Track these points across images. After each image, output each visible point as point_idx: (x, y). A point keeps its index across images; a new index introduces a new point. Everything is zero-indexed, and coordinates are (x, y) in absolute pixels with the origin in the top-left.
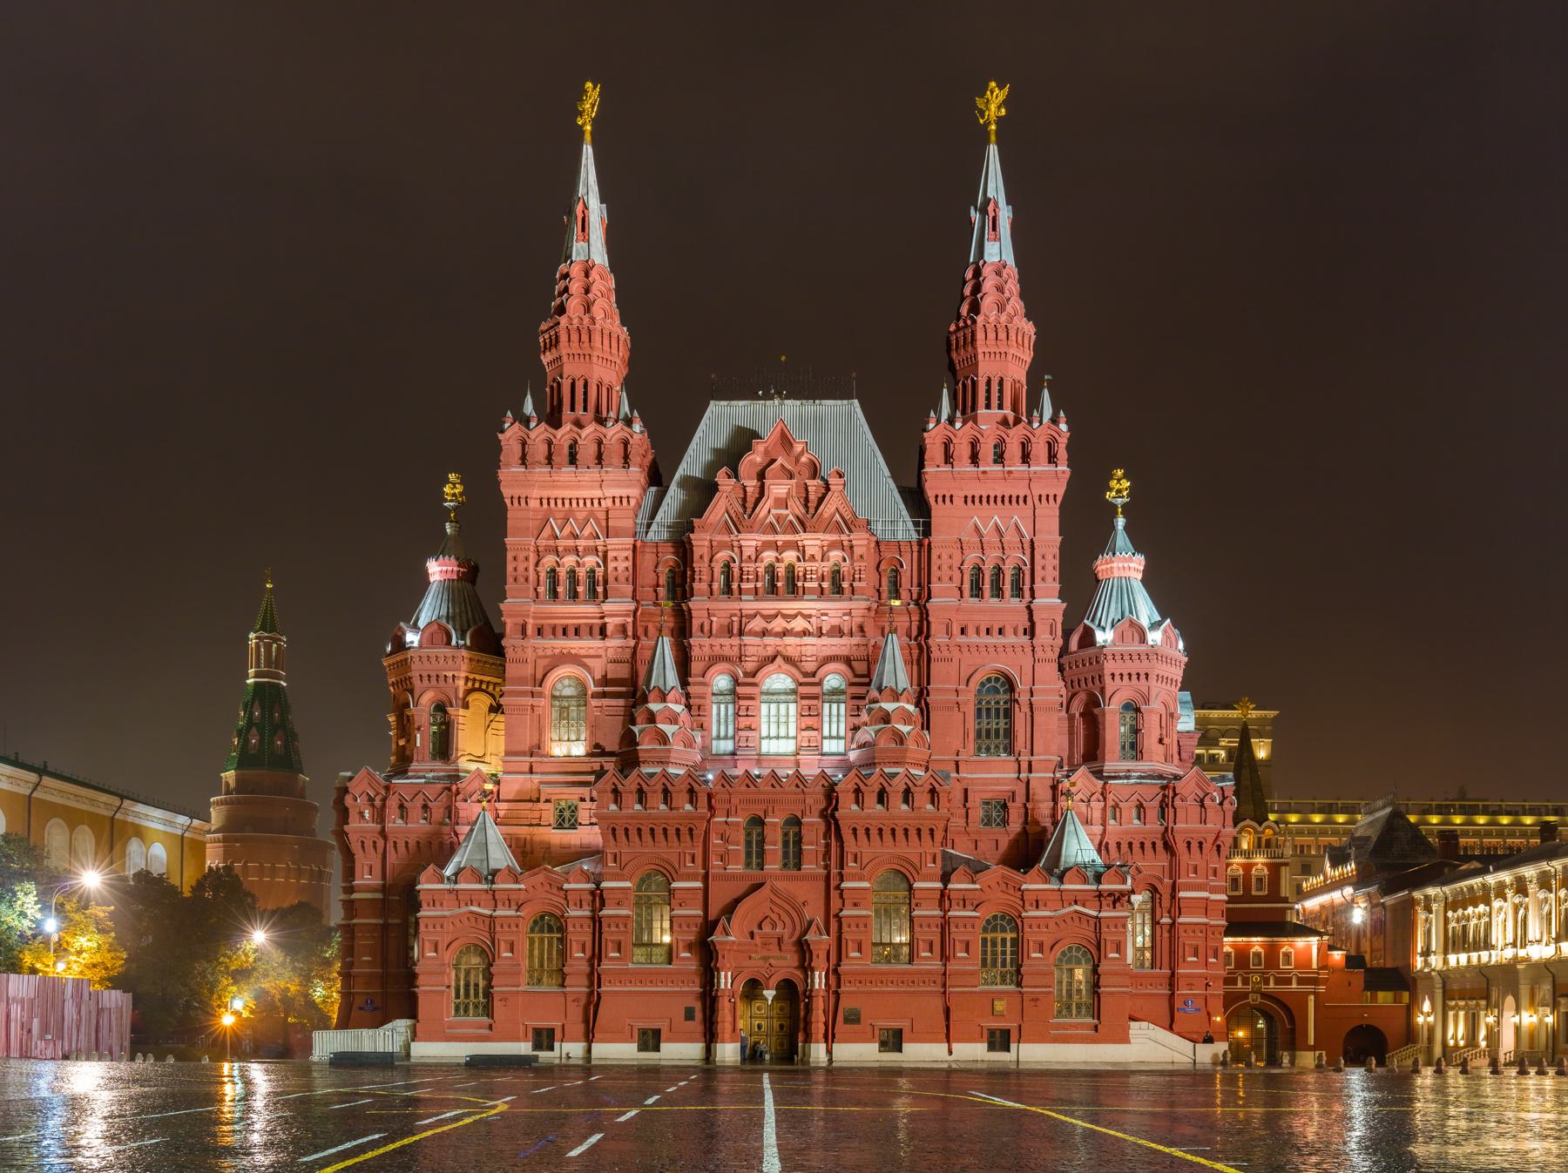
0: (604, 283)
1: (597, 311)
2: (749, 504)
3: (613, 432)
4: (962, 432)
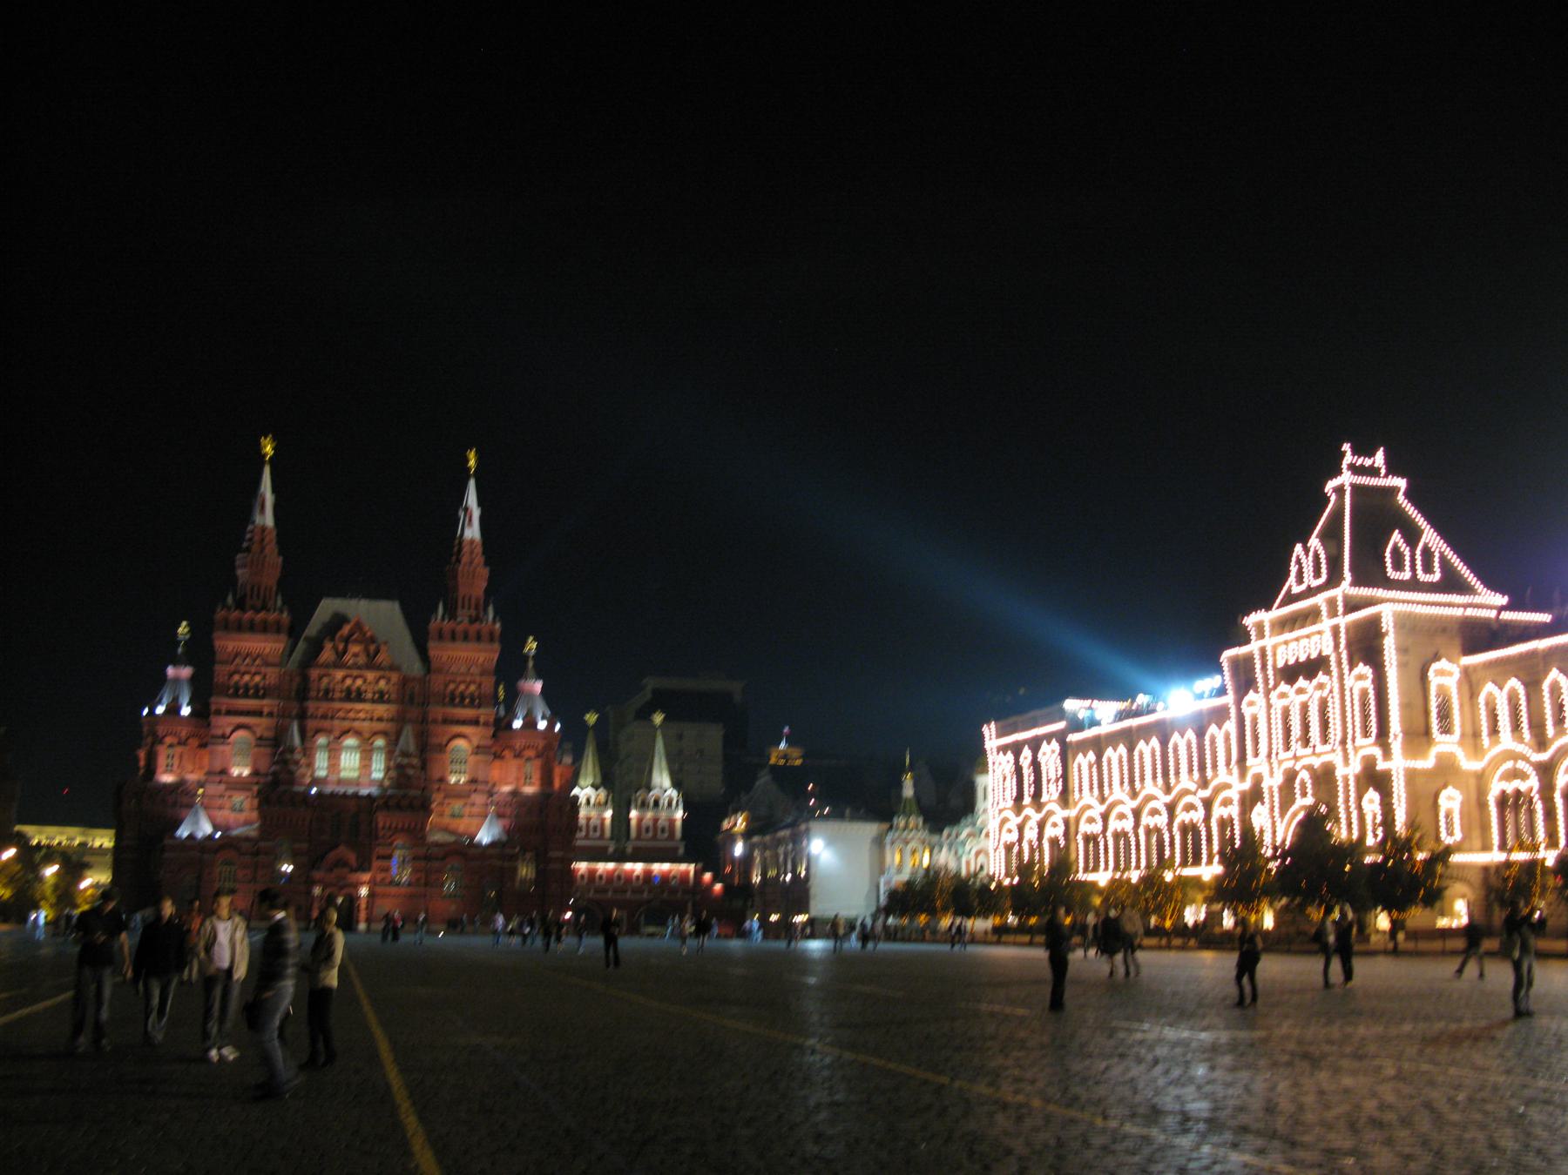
0: (272, 537)
1: (267, 551)
2: (341, 654)
3: (272, 616)
4: (447, 625)
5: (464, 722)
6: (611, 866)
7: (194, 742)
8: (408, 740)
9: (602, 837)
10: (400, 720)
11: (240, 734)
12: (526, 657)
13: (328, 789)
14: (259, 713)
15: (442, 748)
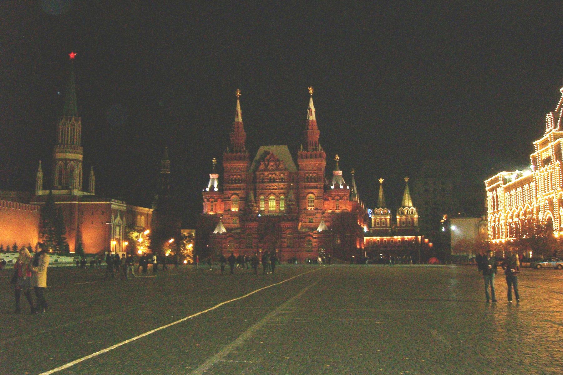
5: (312, 188)
6: (389, 237)
7: (220, 200)
8: (292, 196)
9: (386, 227)
10: (289, 188)
11: (234, 196)
12: (336, 161)
13: (266, 214)
14: (240, 189)
15: (304, 198)
